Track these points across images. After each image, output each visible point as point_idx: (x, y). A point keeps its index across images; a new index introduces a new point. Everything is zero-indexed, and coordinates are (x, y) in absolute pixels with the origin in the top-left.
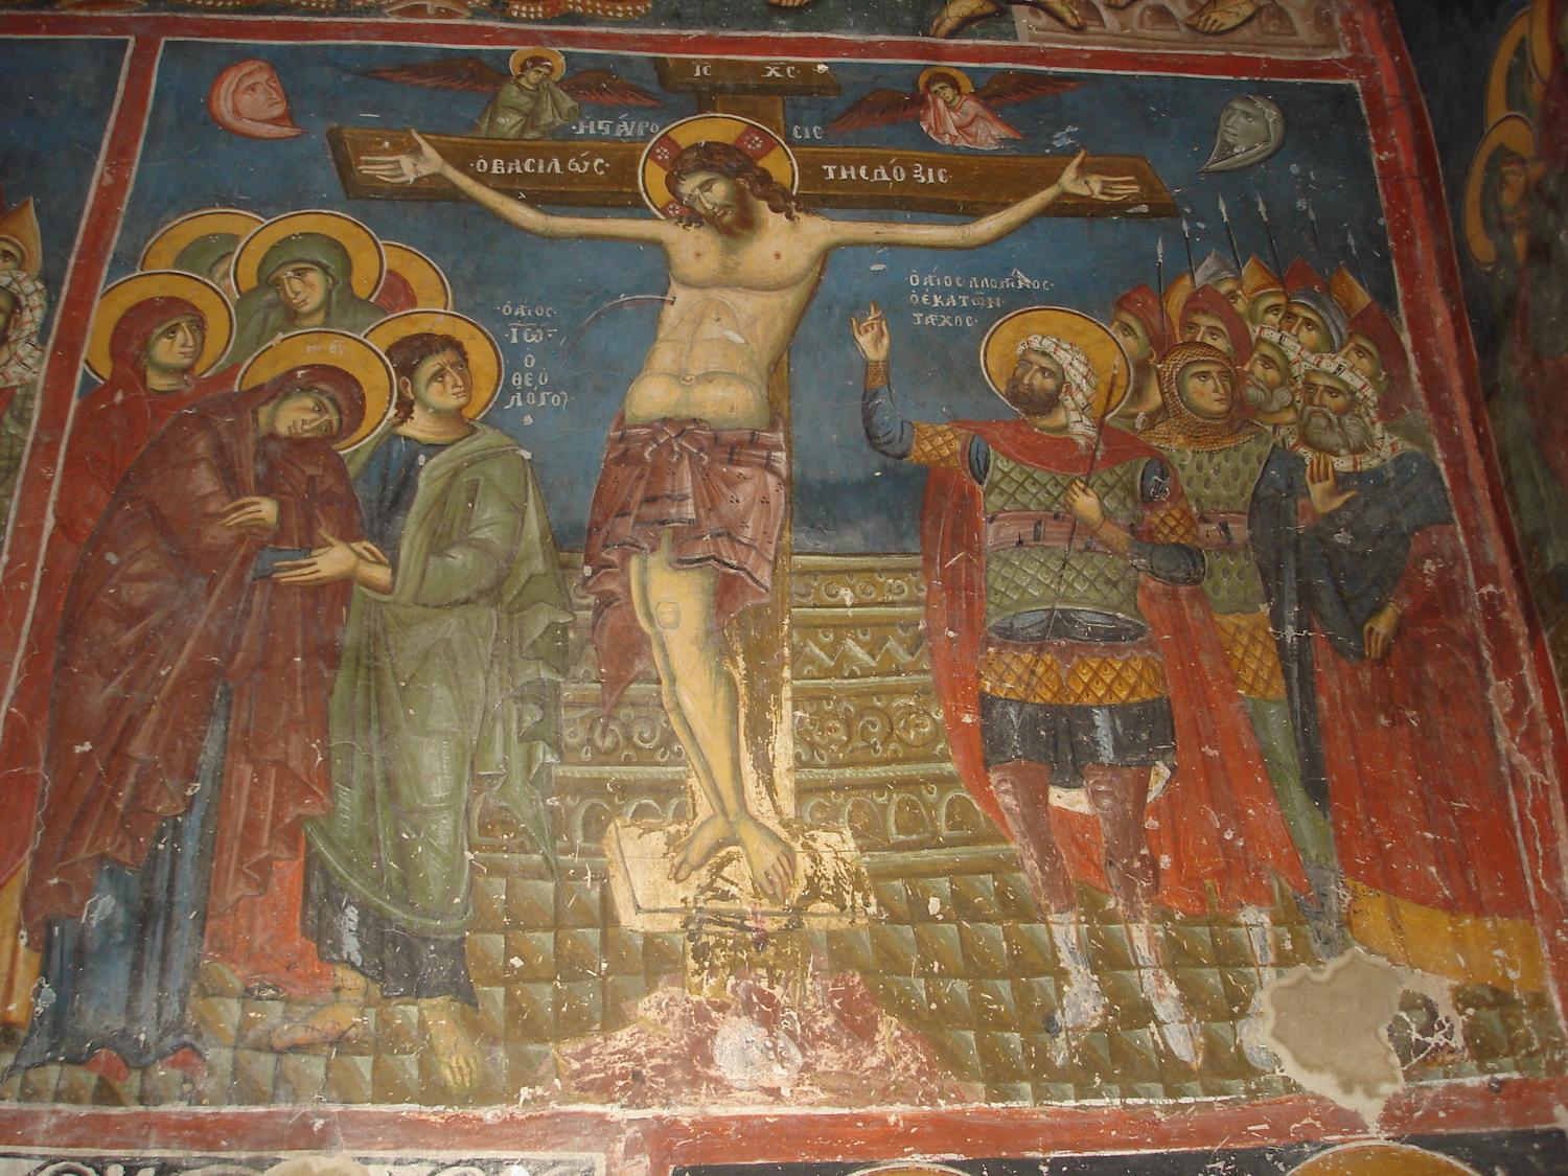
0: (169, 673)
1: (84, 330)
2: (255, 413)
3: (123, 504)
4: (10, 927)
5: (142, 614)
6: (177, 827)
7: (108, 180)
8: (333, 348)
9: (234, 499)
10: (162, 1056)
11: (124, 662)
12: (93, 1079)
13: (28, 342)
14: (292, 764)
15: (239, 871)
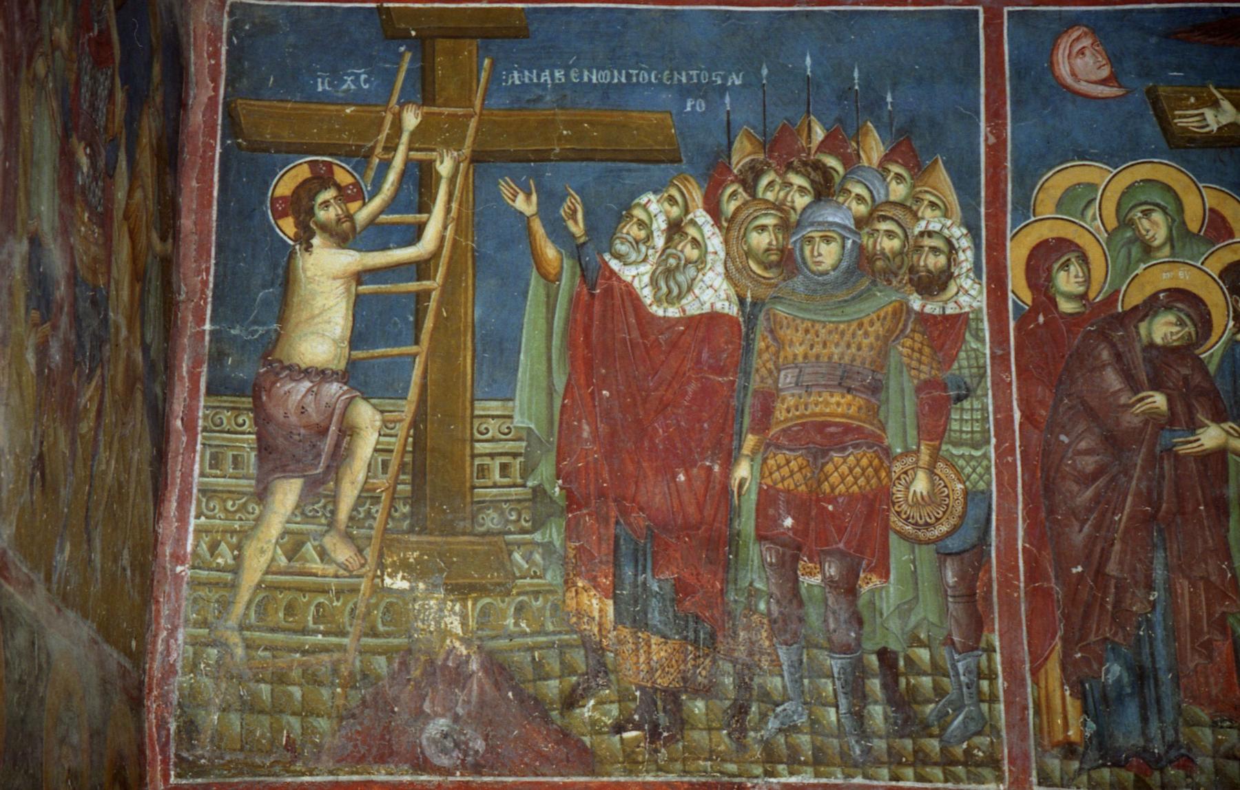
0: (1120, 519)
1: (1005, 267)
2: (1136, 327)
3: (1062, 400)
4: (1057, 684)
5: (1095, 476)
6: (1148, 620)
7: (992, 140)
8: (1181, 274)
9: (1136, 394)
10: (1171, 762)
11: (1090, 510)
12: (1131, 775)
13: (967, 277)
14: (1213, 578)
15: (1193, 648)
